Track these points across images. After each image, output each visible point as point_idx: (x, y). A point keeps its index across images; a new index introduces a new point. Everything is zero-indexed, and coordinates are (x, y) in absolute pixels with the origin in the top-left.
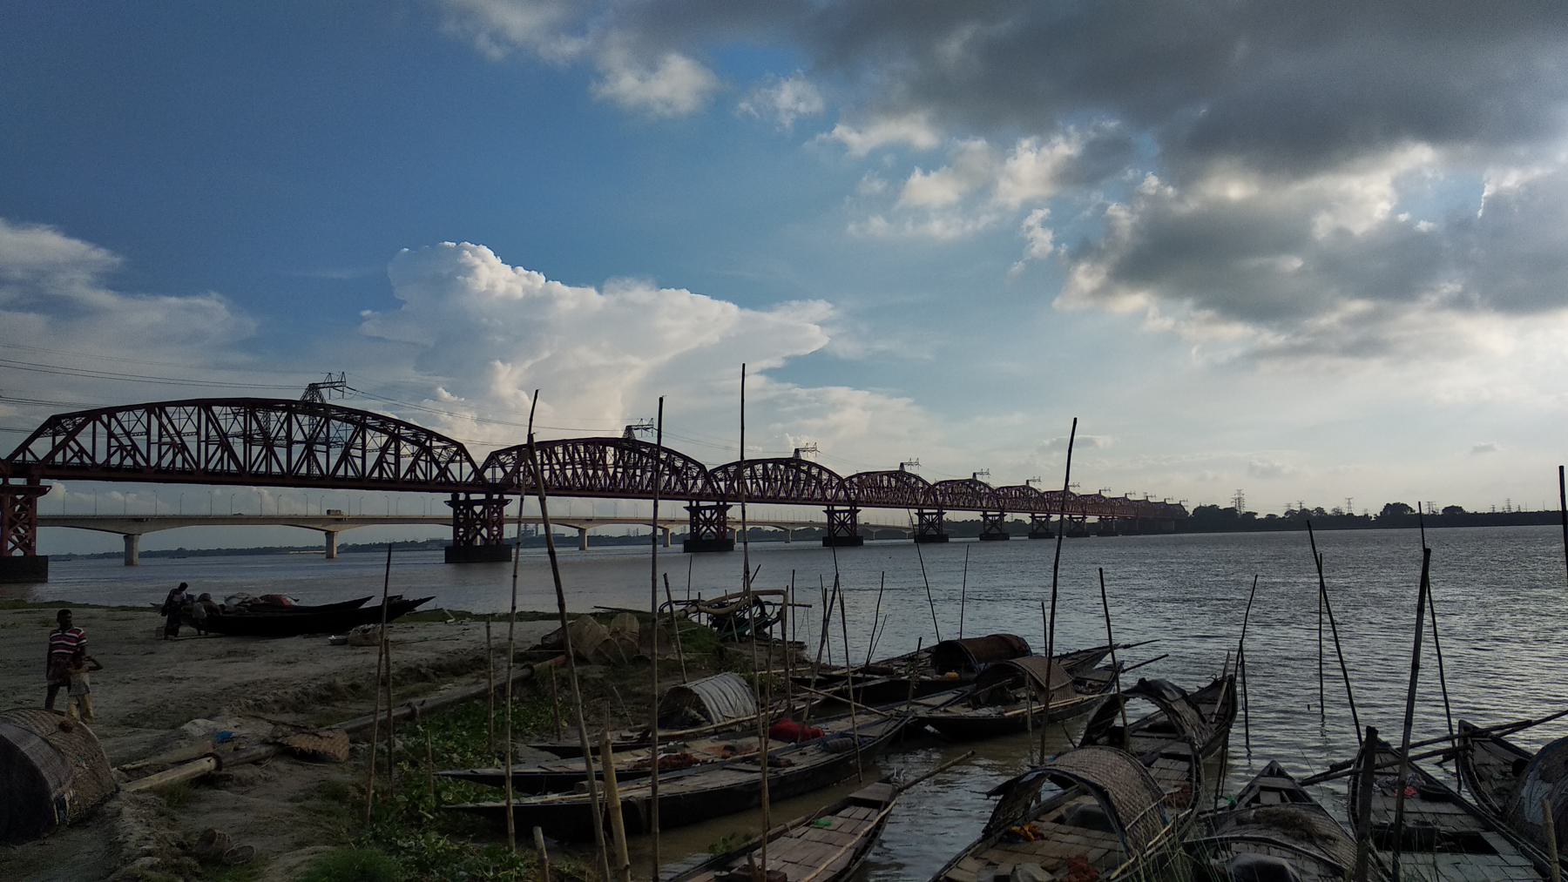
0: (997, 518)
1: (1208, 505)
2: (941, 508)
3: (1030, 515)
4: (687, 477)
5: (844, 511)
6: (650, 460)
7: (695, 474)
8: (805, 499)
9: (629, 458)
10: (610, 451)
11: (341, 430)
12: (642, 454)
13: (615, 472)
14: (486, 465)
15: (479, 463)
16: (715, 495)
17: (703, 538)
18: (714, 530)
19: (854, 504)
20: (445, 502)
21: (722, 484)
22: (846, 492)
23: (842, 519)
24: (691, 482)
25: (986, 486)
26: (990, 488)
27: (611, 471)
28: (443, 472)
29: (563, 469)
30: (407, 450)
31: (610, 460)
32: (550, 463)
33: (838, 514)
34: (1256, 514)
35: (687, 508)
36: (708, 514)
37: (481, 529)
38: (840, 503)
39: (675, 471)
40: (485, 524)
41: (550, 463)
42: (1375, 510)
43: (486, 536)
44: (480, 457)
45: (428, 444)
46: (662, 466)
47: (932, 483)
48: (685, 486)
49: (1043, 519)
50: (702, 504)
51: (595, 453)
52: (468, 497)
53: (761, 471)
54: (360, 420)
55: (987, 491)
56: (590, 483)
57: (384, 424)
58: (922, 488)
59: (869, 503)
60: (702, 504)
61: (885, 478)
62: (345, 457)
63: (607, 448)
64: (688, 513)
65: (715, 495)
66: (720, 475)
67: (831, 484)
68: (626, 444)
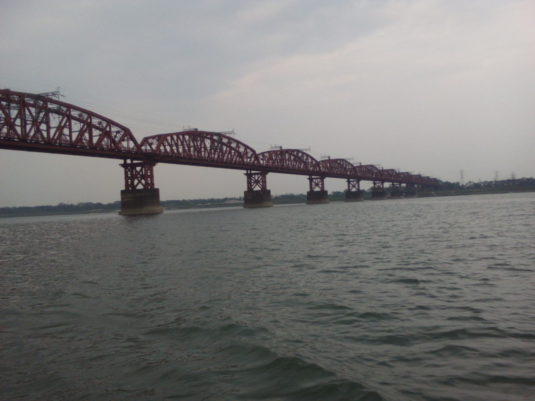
15: (139, 142)
20: (120, 165)
45: (108, 129)
50: (253, 172)
58: (311, 162)
60: (253, 172)
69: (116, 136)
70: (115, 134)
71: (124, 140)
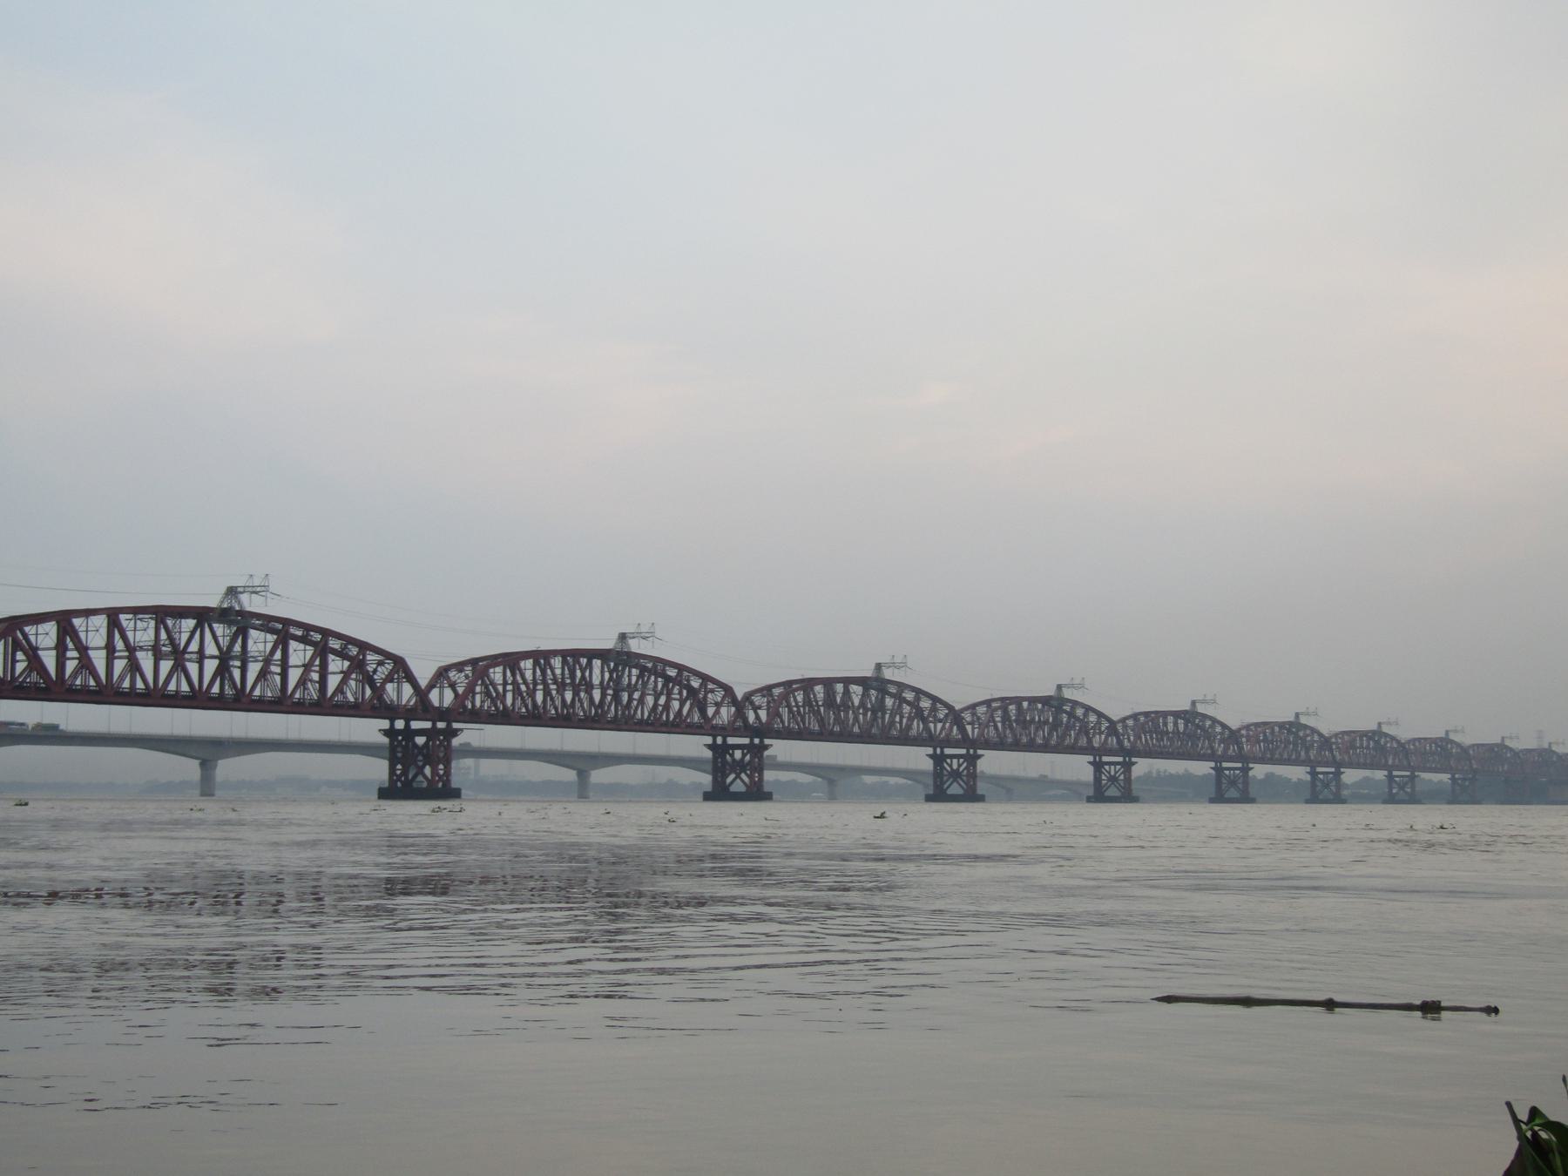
3: (1308, 769)
5: (1118, 763)
6: (653, 678)
7: (719, 699)
10: (597, 663)
11: (259, 642)
12: (643, 669)
16: (748, 730)
17: (415, 785)
20: (380, 730)
22: (1118, 738)
23: (1112, 773)
24: (711, 711)
28: (378, 691)
29: (532, 693)
30: (336, 665)
33: (949, 761)
35: (386, 733)
37: (424, 767)
38: (1111, 753)
39: (692, 692)
41: (544, 682)
43: (430, 777)
46: (671, 685)
48: (703, 711)
50: (731, 741)
52: (724, 741)
53: (822, 695)
54: (283, 630)
56: (596, 712)
57: (307, 633)
58: (1220, 733)
59: (1149, 754)
61: (1170, 719)
62: (263, 674)
63: (594, 661)
64: (931, 762)
65: (965, 741)
67: (1100, 729)
68: (619, 657)
69: (375, 671)
70: (374, 666)
71: (391, 681)
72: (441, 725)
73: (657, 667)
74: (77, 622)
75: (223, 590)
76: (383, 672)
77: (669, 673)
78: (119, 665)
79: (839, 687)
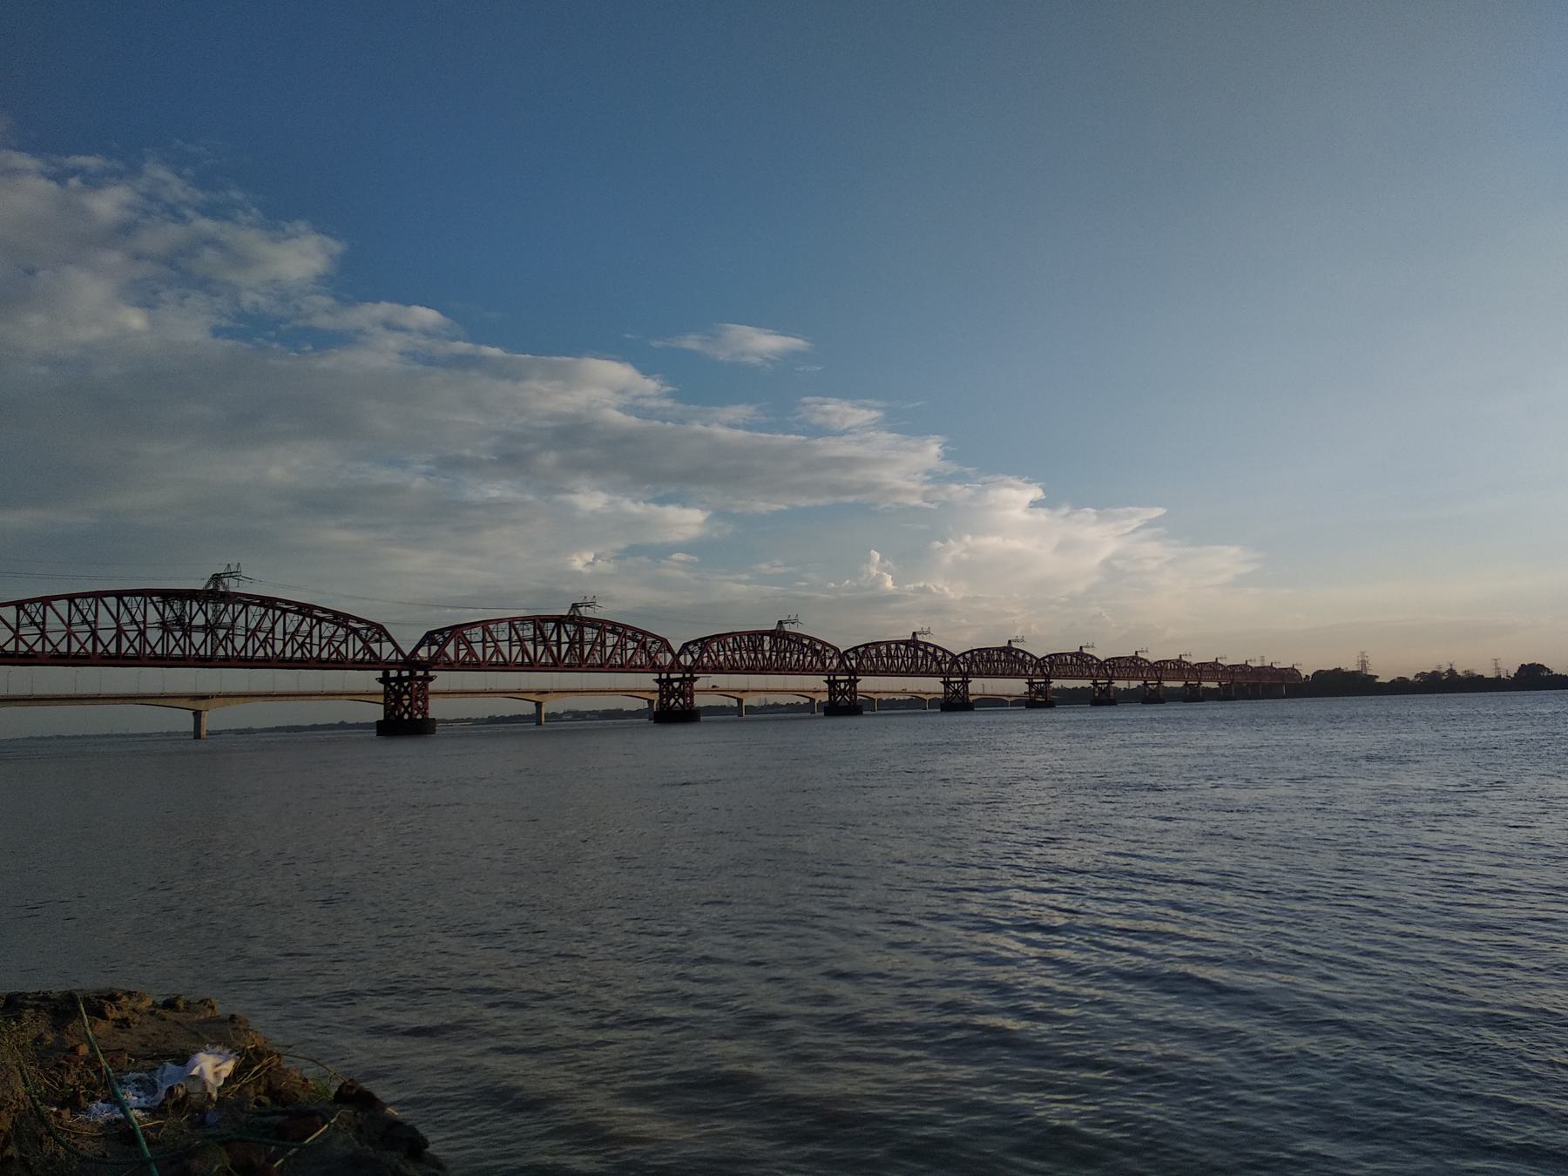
0: (1155, 686)
1: (1331, 669)
2: (1111, 678)
4: (825, 658)
8: (913, 672)
9: (780, 645)
10: (767, 638)
12: (790, 641)
13: (771, 655)
14: (681, 653)
18: (848, 700)
19: (966, 676)
21: (854, 662)
24: (828, 662)
25: (1146, 661)
26: (1149, 663)
27: (767, 654)
31: (766, 646)
32: (724, 651)
34: (1377, 677)
36: (842, 685)
39: (816, 653)
40: (682, 695)
41: (724, 651)
42: (1510, 669)
44: (676, 648)
46: (806, 649)
47: (1103, 660)
48: (823, 664)
49: (1155, 686)
51: (756, 642)
55: (1147, 665)
60: (838, 678)
63: (765, 637)
66: (851, 655)
68: (778, 634)
69: (650, 647)
72: (687, 675)
73: (800, 637)
74: (491, 626)
75: (570, 607)
76: (655, 647)
77: (804, 642)
78: (516, 650)
79: (893, 646)
